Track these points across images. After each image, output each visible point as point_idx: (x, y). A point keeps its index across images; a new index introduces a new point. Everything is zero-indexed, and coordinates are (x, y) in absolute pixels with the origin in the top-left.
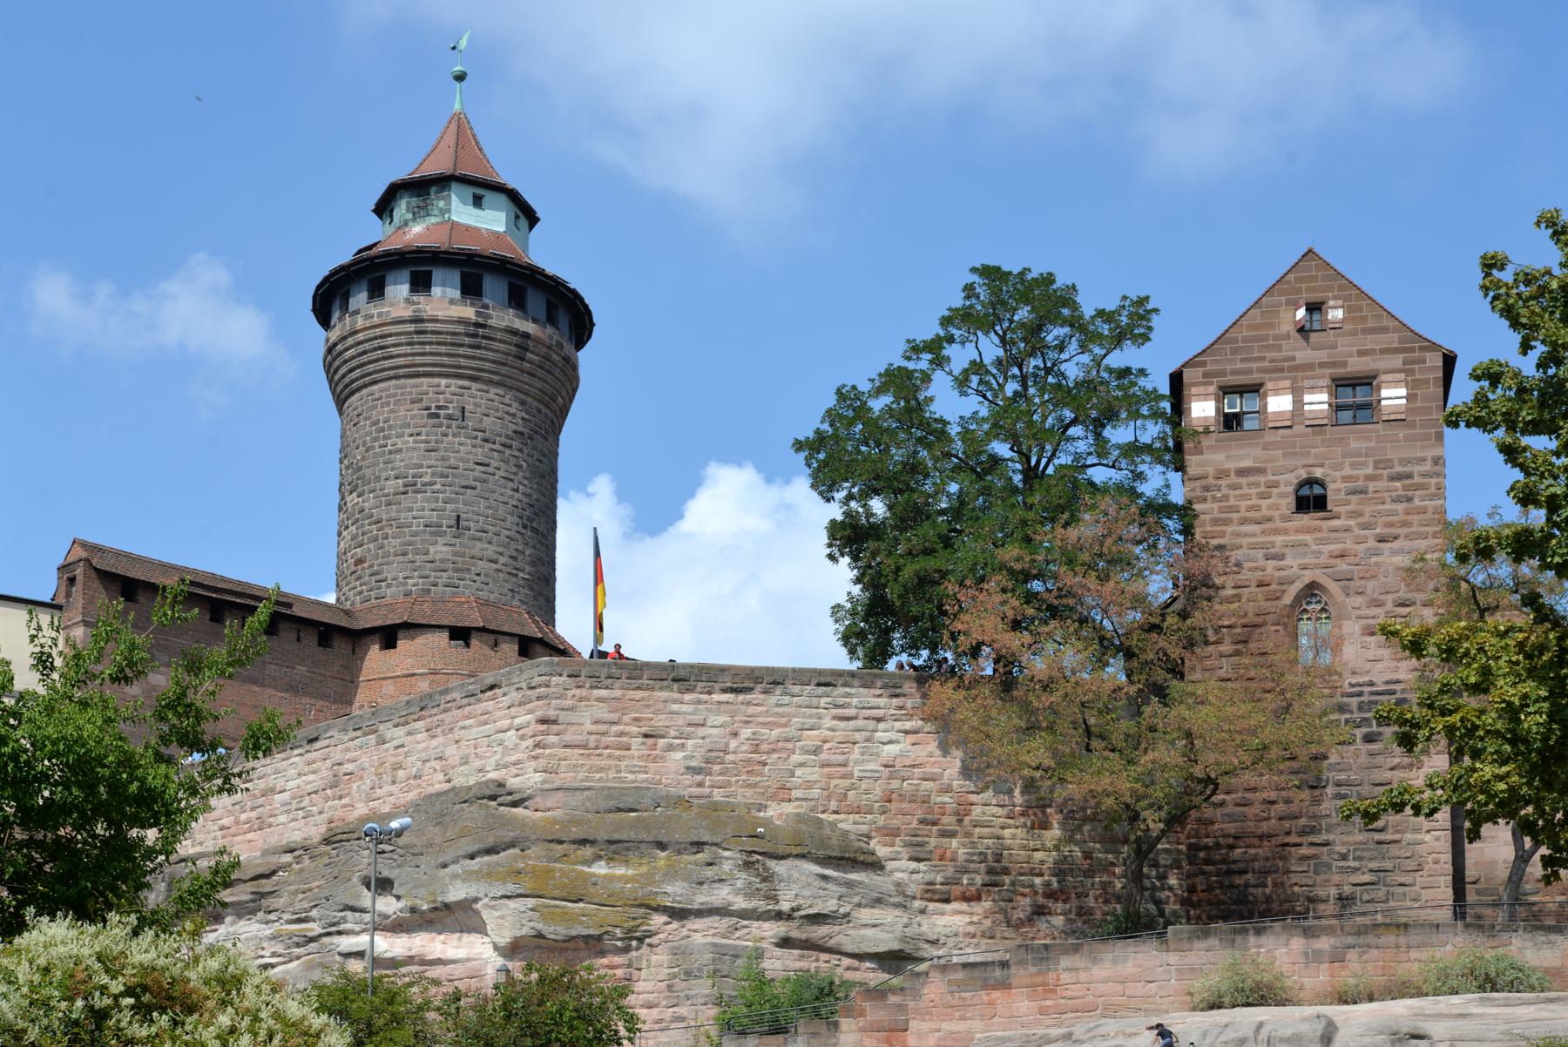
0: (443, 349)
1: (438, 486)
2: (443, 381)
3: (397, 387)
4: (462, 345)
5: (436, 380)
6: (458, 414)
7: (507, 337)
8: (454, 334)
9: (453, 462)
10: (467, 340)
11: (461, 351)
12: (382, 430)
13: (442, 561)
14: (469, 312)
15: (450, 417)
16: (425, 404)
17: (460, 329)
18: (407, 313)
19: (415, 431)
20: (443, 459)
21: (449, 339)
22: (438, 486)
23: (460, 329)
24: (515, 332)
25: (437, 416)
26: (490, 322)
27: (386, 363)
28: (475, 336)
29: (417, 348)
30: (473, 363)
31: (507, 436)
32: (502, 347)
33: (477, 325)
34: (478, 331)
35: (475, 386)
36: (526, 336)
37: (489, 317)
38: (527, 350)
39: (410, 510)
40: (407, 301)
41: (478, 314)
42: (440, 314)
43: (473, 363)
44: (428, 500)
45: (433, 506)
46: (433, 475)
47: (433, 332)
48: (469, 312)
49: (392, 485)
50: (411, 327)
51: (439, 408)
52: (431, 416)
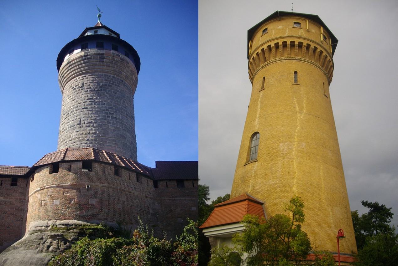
0: (76, 68)
1: (75, 112)
2: (78, 78)
4: (81, 64)
5: (76, 78)
8: (79, 61)
11: (81, 66)
13: (75, 138)
16: (72, 87)
24: (98, 54)
28: (85, 59)
36: (103, 54)
38: (104, 58)
39: (67, 123)
44: (71, 118)
47: (73, 64)
50: (68, 66)
52: (73, 90)
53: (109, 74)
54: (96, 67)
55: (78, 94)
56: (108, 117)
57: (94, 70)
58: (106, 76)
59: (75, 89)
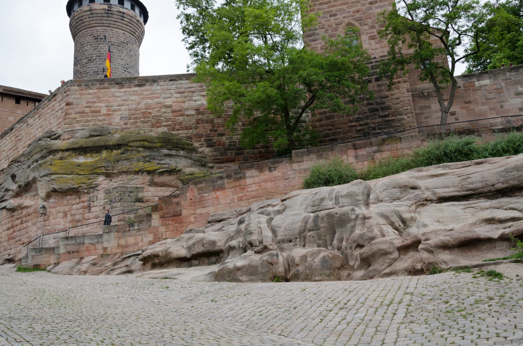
1: (98, 60)
2: (99, 28)
3: (86, 31)
5: (97, 28)
6: (104, 38)
7: (118, 13)
9: (102, 52)
10: (105, 15)
11: (104, 18)
12: (82, 45)
14: (106, 7)
15: (101, 39)
16: (94, 35)
17: (103, 11)
18: (88, 9)
19: (90, 44)
20: (99, 51)
21: (100, 15)
22: (98, 60)
23: (103, 11)
25: (97, 39)
26: (112, 9)
27: (83, 25)
28: (108, 13)
29: (91, 19)
30: (107, 22)
31: (119, 44)
32: (116, 17)
33: (108, 10)
34: (109, 12)
35: (108, 28)
37: (112, 8)
39: (89, 68)
40: (88, 5)
41: (108, 7)
42: (97, 8)
43: (107, 22)
44: (95, 64)
45: (96, 66)
46: (96, 56)
48: (106, 7)
49: (85, 61)
50: (89, 13)
51: (98, 36)
52: (95, 39)
53: (126, 33)
54: (117, 24)
55: (99, 44)
56: (125, 71)
57: (115, 26)
58: (124, 34)
59: (97, 39)
